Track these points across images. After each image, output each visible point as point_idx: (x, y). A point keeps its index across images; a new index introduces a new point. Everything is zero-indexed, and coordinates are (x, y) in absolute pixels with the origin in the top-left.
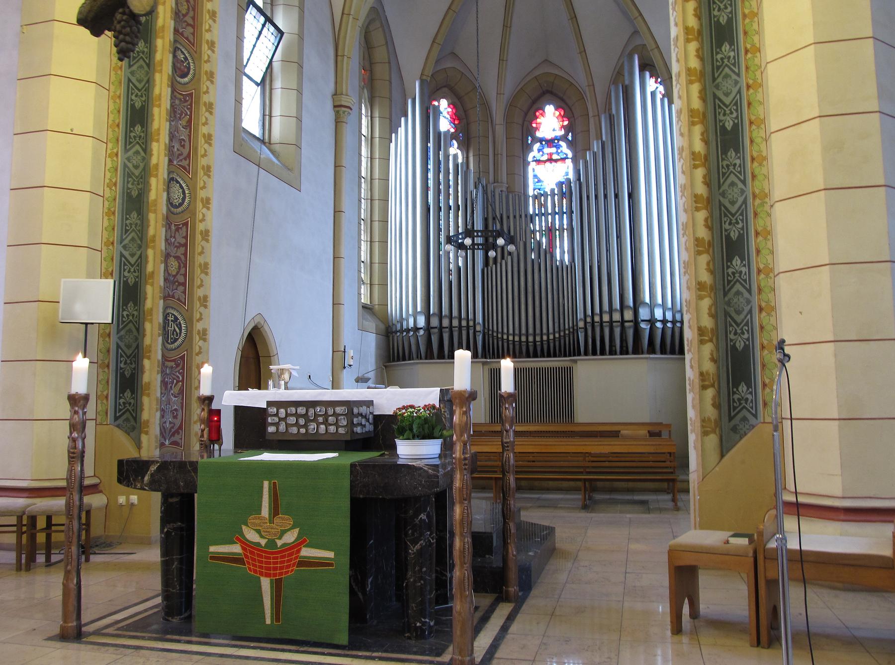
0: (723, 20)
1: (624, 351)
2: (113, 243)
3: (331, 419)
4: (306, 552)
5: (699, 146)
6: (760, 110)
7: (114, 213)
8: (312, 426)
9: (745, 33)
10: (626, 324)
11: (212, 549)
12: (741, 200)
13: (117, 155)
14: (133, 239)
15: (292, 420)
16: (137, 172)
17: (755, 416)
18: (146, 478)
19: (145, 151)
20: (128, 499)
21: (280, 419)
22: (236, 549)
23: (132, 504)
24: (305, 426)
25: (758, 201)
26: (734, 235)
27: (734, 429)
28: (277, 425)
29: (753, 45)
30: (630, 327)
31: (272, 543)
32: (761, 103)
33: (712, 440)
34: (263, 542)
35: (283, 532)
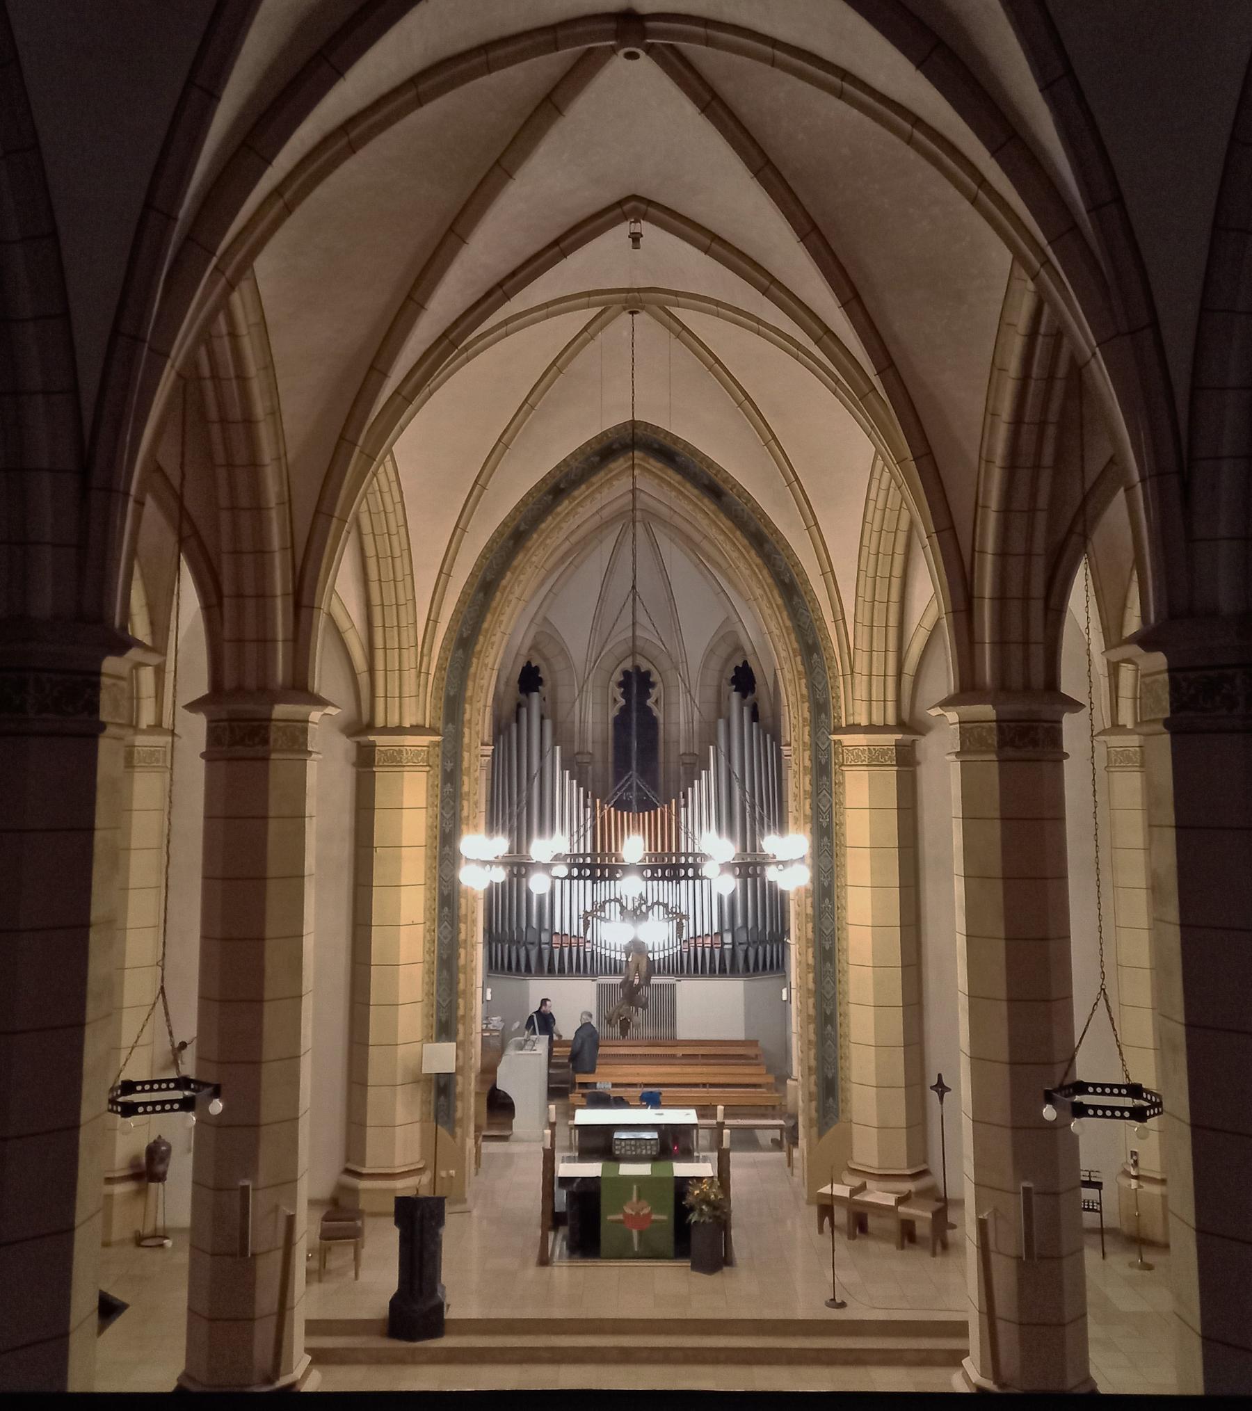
0: (826, 884)
1: (723, 972)
2: (432, 994)
3: (648, 1147)
4: (654, 1217)
5: (811, 961)
6: (844, 943)
7: (433, 973)
8: (639, 1151)
9: (838, 897)
10: (726, 946)
11: (611, 1217)
12: (833, 992)
13: (434, 931)
14: (444, 989)
15: (628, 1148)
16: (446, 942)
17: (837, 1117)
18: (575, 1185)
19: (452, 926)
20: (448, 1174)
21: (622, 1147)
22: (621, 1217)
23: (452, 1177)
24: (635, 1150)
25: (841, 996)
26: (828, 1013)
27: (826, 1124)
28: (620, 1150)
29: (842, 905)
30: (729, 949)
31: (638, 1214)
32: (843, 876)
33: (815, 1130)
34: (634, 1213)
35: (643, 1209)
